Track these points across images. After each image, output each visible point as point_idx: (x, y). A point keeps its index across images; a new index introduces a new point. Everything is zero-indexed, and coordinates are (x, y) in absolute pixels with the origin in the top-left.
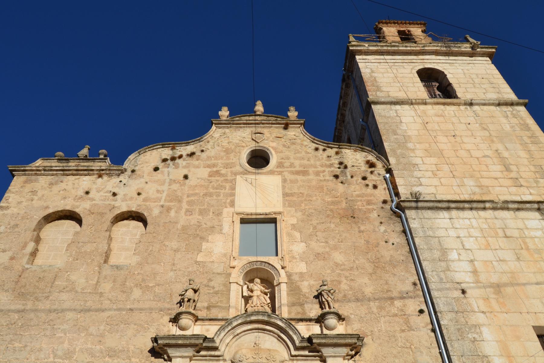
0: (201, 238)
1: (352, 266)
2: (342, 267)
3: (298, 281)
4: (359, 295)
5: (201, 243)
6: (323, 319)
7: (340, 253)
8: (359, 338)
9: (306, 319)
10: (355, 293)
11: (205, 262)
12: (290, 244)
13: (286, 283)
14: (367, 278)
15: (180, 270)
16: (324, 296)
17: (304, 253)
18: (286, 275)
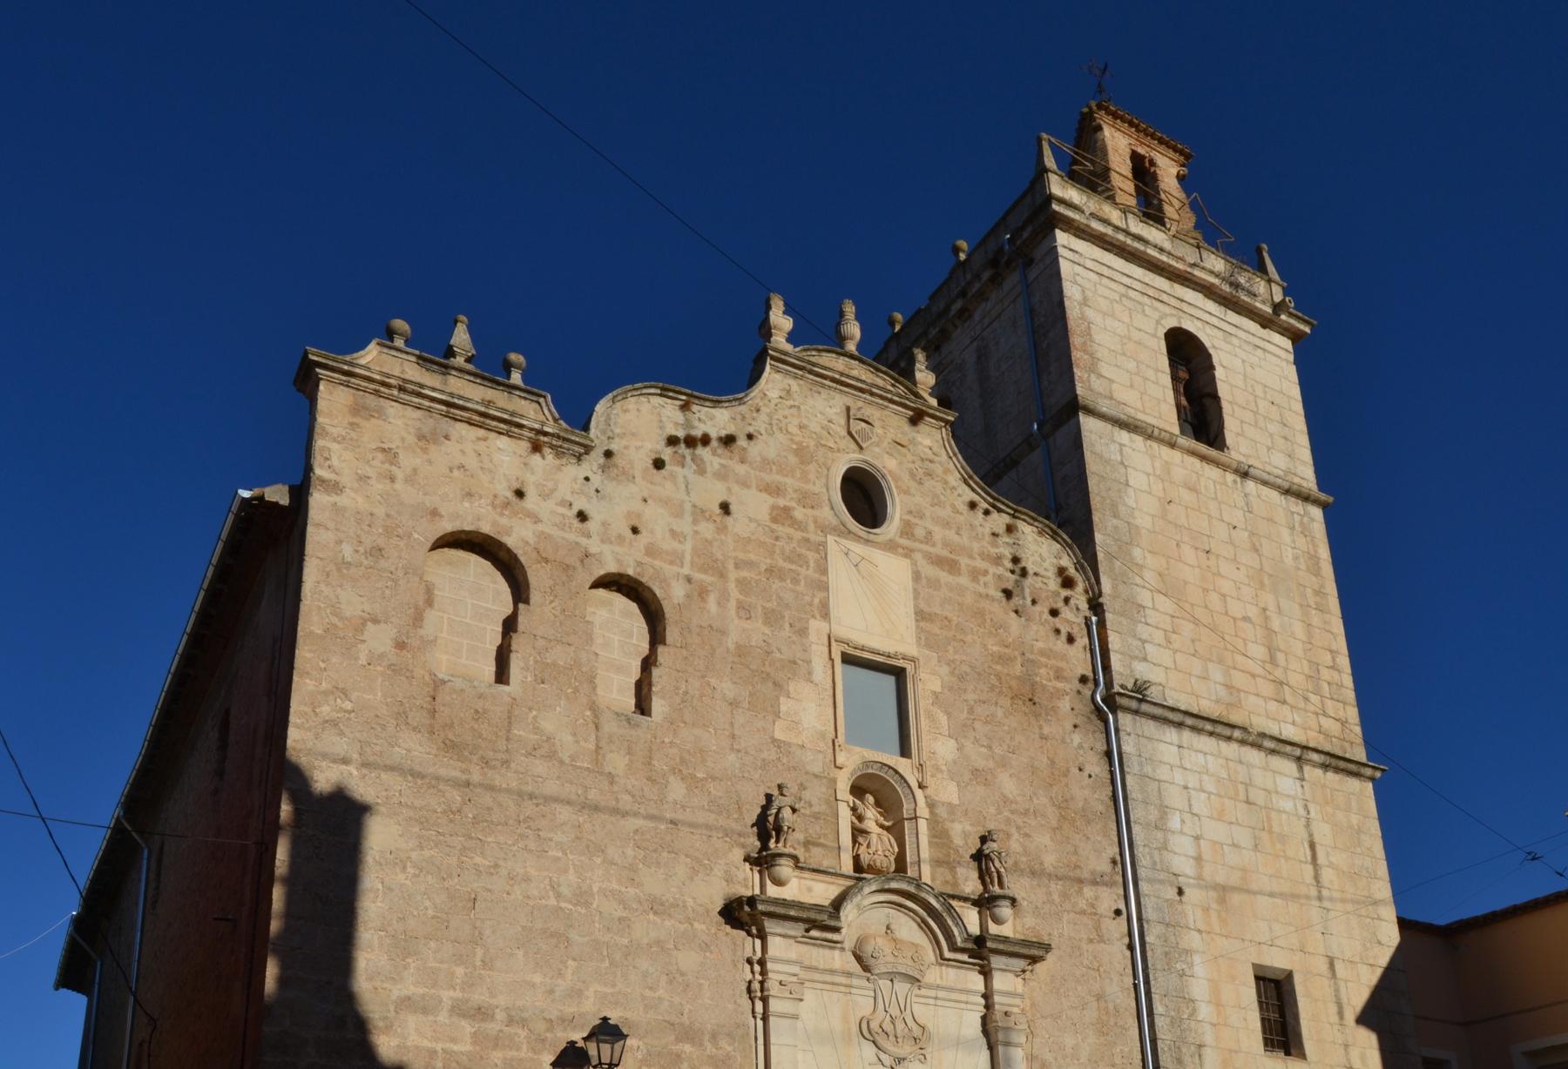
0: (775, 684)
5: (777, 698)
6: (989, 903)
7: (1010, 776)
11: (790, 745)
15: (746, 753)
17: (955, 762)
18: (927, 802)
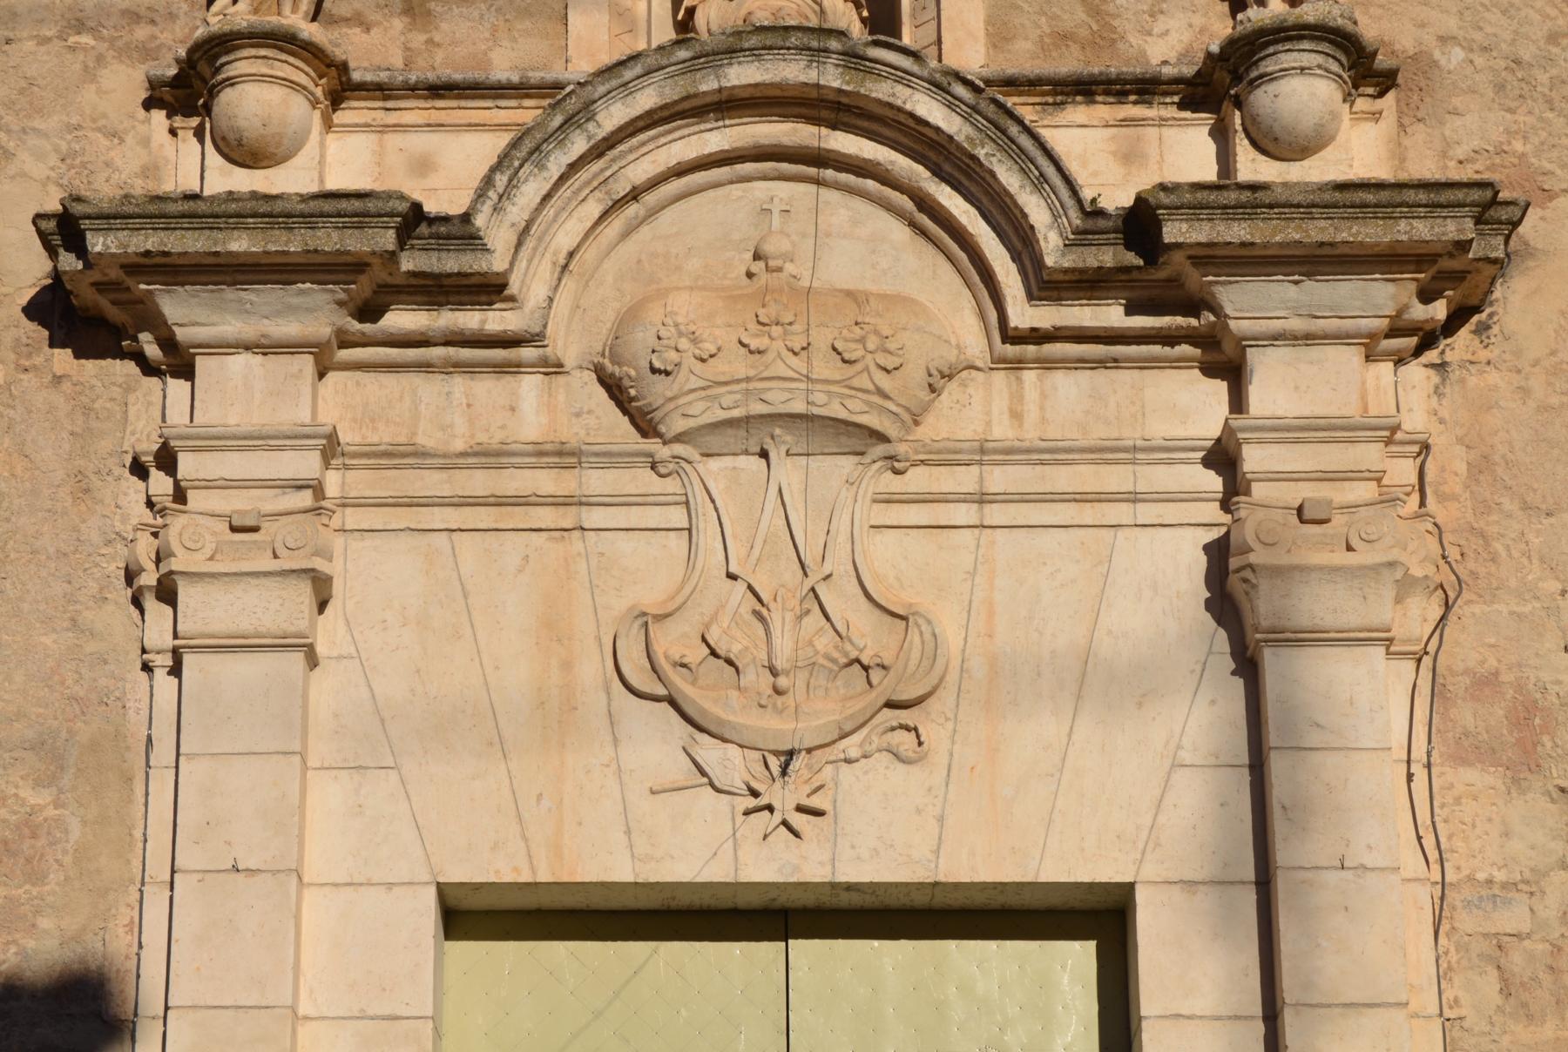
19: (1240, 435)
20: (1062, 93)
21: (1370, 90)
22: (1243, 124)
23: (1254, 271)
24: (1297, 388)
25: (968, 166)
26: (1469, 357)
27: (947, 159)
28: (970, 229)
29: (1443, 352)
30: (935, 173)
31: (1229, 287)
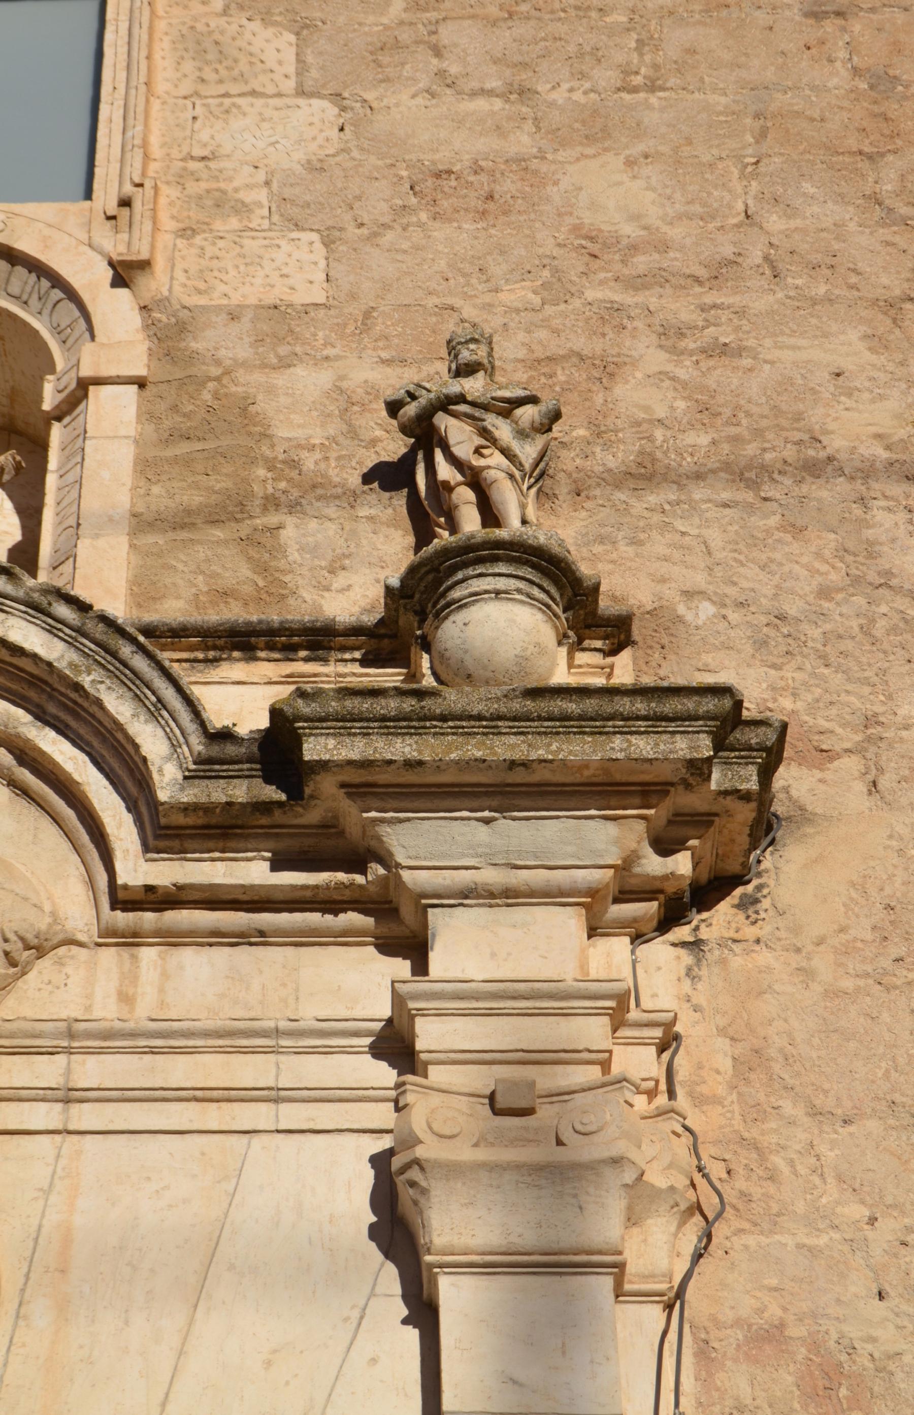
1: (728, 251)
2: (641, 262)
3: (244, 364)
4: (768, 456)
7: (630, 163)
8: (739, 735)
9: (284, 630)
10: (735, 440)
12: (199, 111)
13: (141, 383)
14: (853, 335)
16: (452, 439)
17: (316, 167)
18: (150, 326)
19: (412, 1005)
20: (215, 648)
21: (598, 644)
22: (432, 668)
23: (429, 805)
24: (493, 955)
25: (75, 702)
26: (732, 934)
27: (51, 697)
28: (76, 777)
29: (697, 928)
30: (37, 717)
31: (399, 827)
